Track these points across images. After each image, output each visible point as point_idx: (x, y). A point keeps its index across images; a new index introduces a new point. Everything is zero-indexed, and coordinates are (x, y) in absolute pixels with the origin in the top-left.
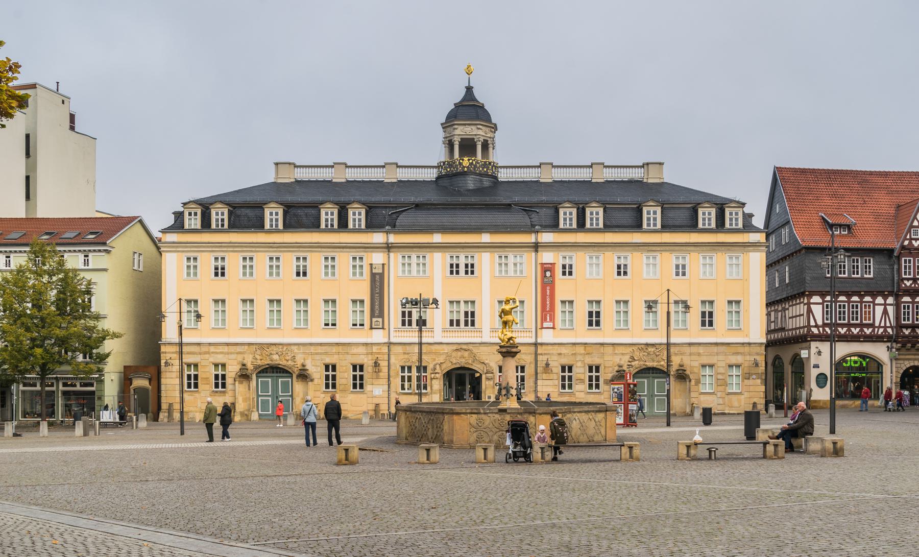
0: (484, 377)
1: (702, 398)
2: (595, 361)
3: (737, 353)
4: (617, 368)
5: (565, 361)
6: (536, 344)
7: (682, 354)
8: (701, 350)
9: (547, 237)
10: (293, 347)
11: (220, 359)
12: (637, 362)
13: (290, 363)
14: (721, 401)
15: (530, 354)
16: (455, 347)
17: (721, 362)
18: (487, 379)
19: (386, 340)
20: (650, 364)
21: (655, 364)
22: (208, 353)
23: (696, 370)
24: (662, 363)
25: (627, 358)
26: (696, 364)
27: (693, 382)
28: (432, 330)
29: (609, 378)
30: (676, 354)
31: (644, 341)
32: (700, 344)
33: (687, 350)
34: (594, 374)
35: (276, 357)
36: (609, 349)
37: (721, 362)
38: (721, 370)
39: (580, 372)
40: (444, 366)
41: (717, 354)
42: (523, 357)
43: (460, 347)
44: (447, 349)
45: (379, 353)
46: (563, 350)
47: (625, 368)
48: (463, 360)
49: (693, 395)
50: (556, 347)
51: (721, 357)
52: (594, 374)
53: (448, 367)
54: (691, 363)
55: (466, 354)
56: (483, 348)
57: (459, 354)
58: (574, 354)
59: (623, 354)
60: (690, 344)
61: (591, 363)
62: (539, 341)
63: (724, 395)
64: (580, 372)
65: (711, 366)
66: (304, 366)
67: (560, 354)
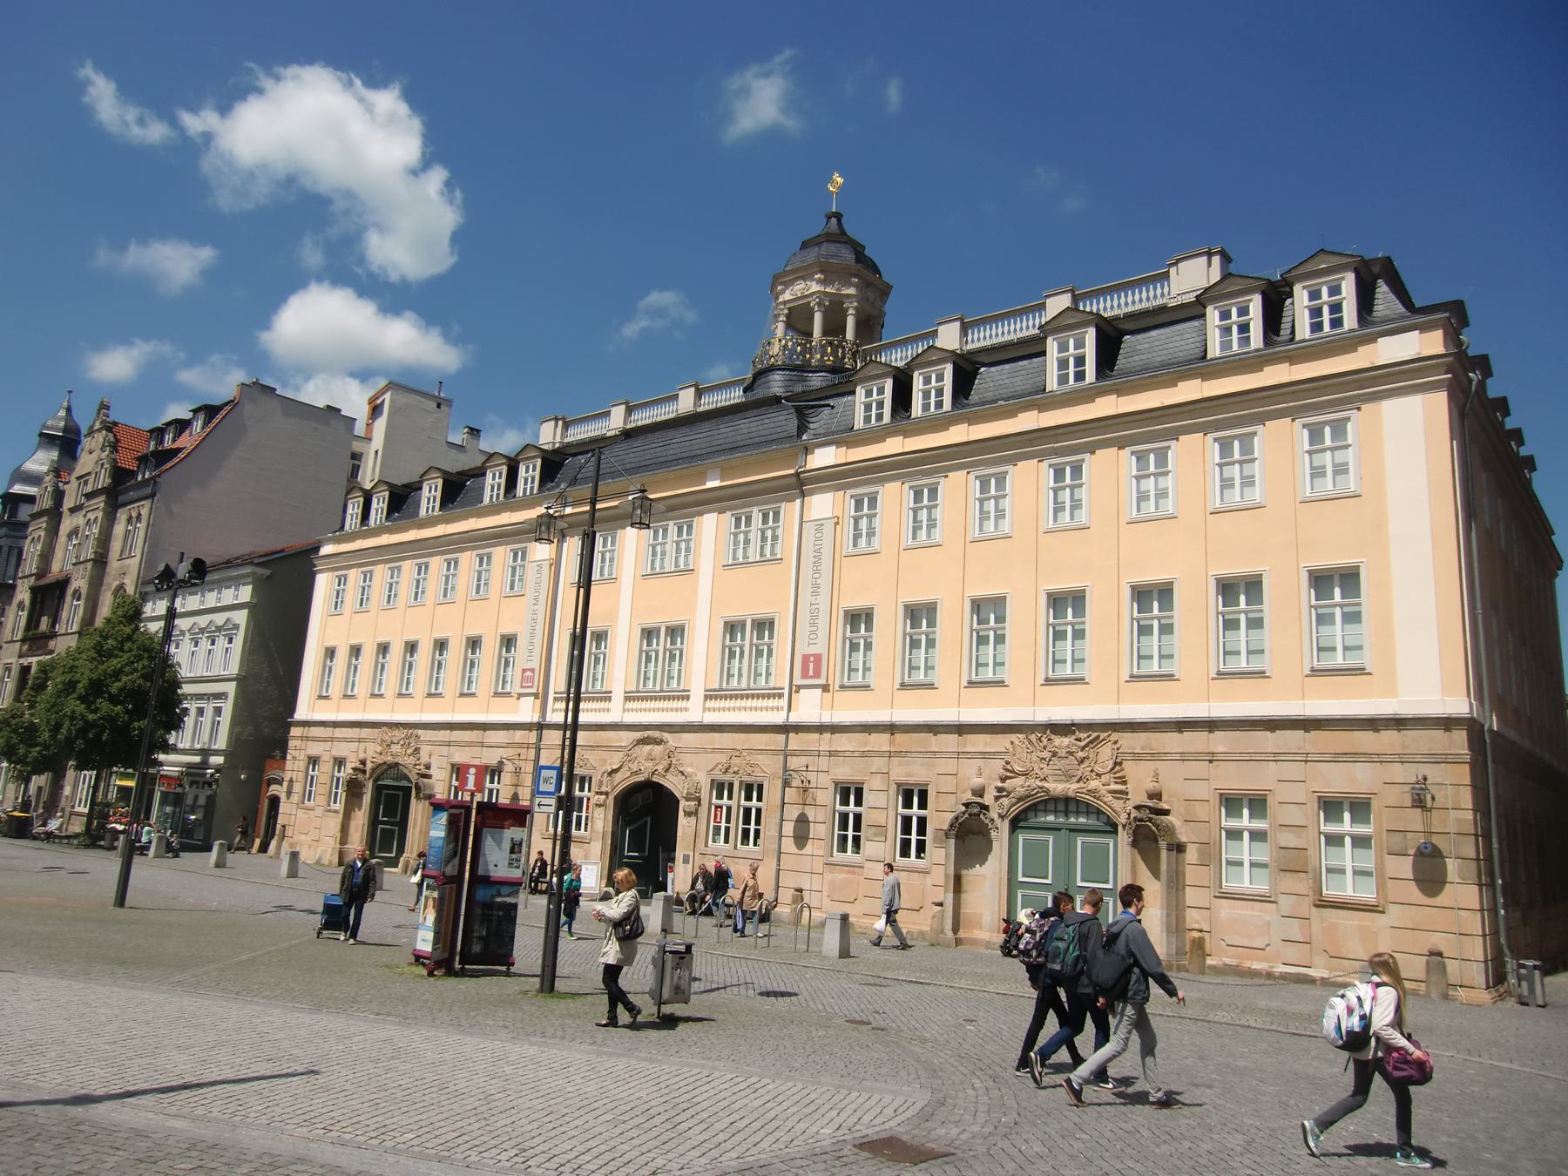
0: (683, 804)
1: (1225, 909)
2: (915, 773)
3: (1354, 757)
4: (968, 796)
5: (846, 772)
6: (785, 729)
7: (1156, 756)
8: (1220, 742)
9: (824, 457)
10: (420, 732)
11: (341, 750)
12: (1019, 781)
13: (410, 761)
14: (1295, 930)
15: (774, 752)
16: (638, 735)
17: (1293, 785)
18: (688, 814)
19: (536, 719)
20: (1057, 788)
21: (1071, 788)
22: (332, 739)
23: (1201, 812)
24: (1093, 784)
25: (997, 766)
26: (1202, 790)
27: (1191, 854)
28: (606, 697)
29: (946, 827)
30: (1137, 757)
31: (1043, 715)
32: (1211, 725)
33: (1172, 742)
34: (915, 810)
35: (396, 748)
36: (950, 741)
37: (1293, 785)
38: (1293, 816)
39: (881, 807)
40: (618, 777)
41: (1277, 757)
42: (762, 760)
43: (649, 734)
44: (627, 738)
45: (520, 745)
46: (843, 742)
47: (988, 799)
48: (649, 764)
49: (1191, 896)
50: (827, 736)
51: (1293, 770)
52: (915, 810)
53: (623, 780)
54: (1189, 791)
55: (658, 749)
56: (689, 739)
57: (647, 748)
58: (865, 754)
59: (984, 755)
60: (1182, 725)
61: (903, 779)
62: (795, 718)
63: (1305, 906)
64: (881, 807)
65: (1258, 804)
66: (428, 767)
67: (832, 754)
